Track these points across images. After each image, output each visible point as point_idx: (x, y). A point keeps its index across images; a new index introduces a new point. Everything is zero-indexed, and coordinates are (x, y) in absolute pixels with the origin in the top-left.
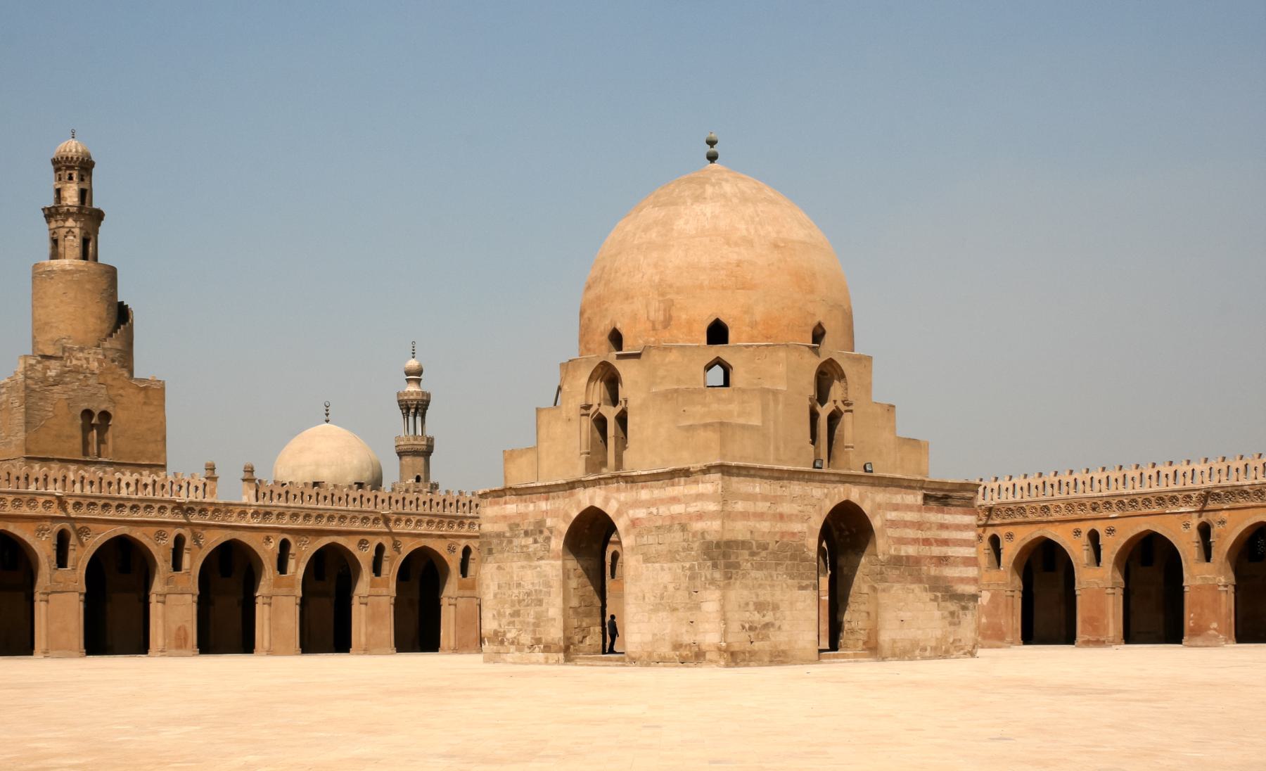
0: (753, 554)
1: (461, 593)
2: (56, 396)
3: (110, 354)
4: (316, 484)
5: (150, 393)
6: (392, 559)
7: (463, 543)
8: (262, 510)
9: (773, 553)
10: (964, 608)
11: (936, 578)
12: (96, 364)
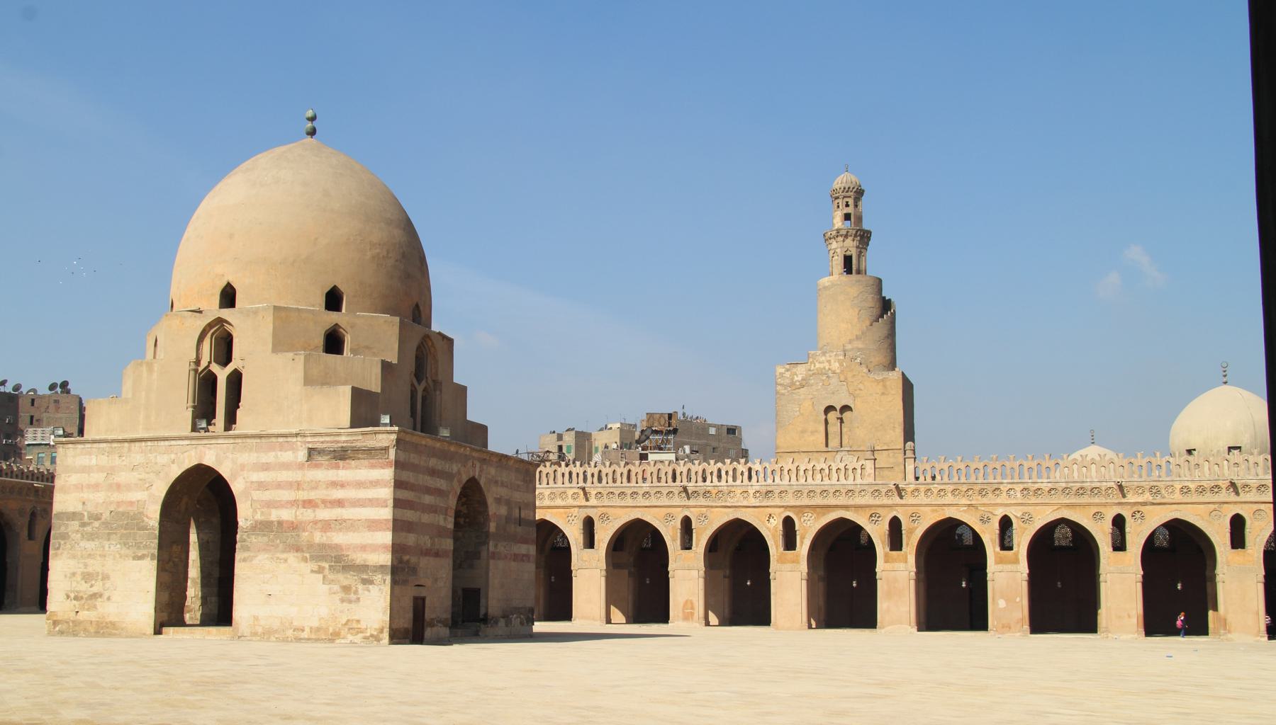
0: (83, 525)
1: (1000, 567)
3: (850, 354)
4: (1190, 452)
6: (911, 531)
7: (1000, 512)
8: (764, 490)
9: (106, 524)
10: (367, 582)
11: (323, 546)
12: (837, 364)
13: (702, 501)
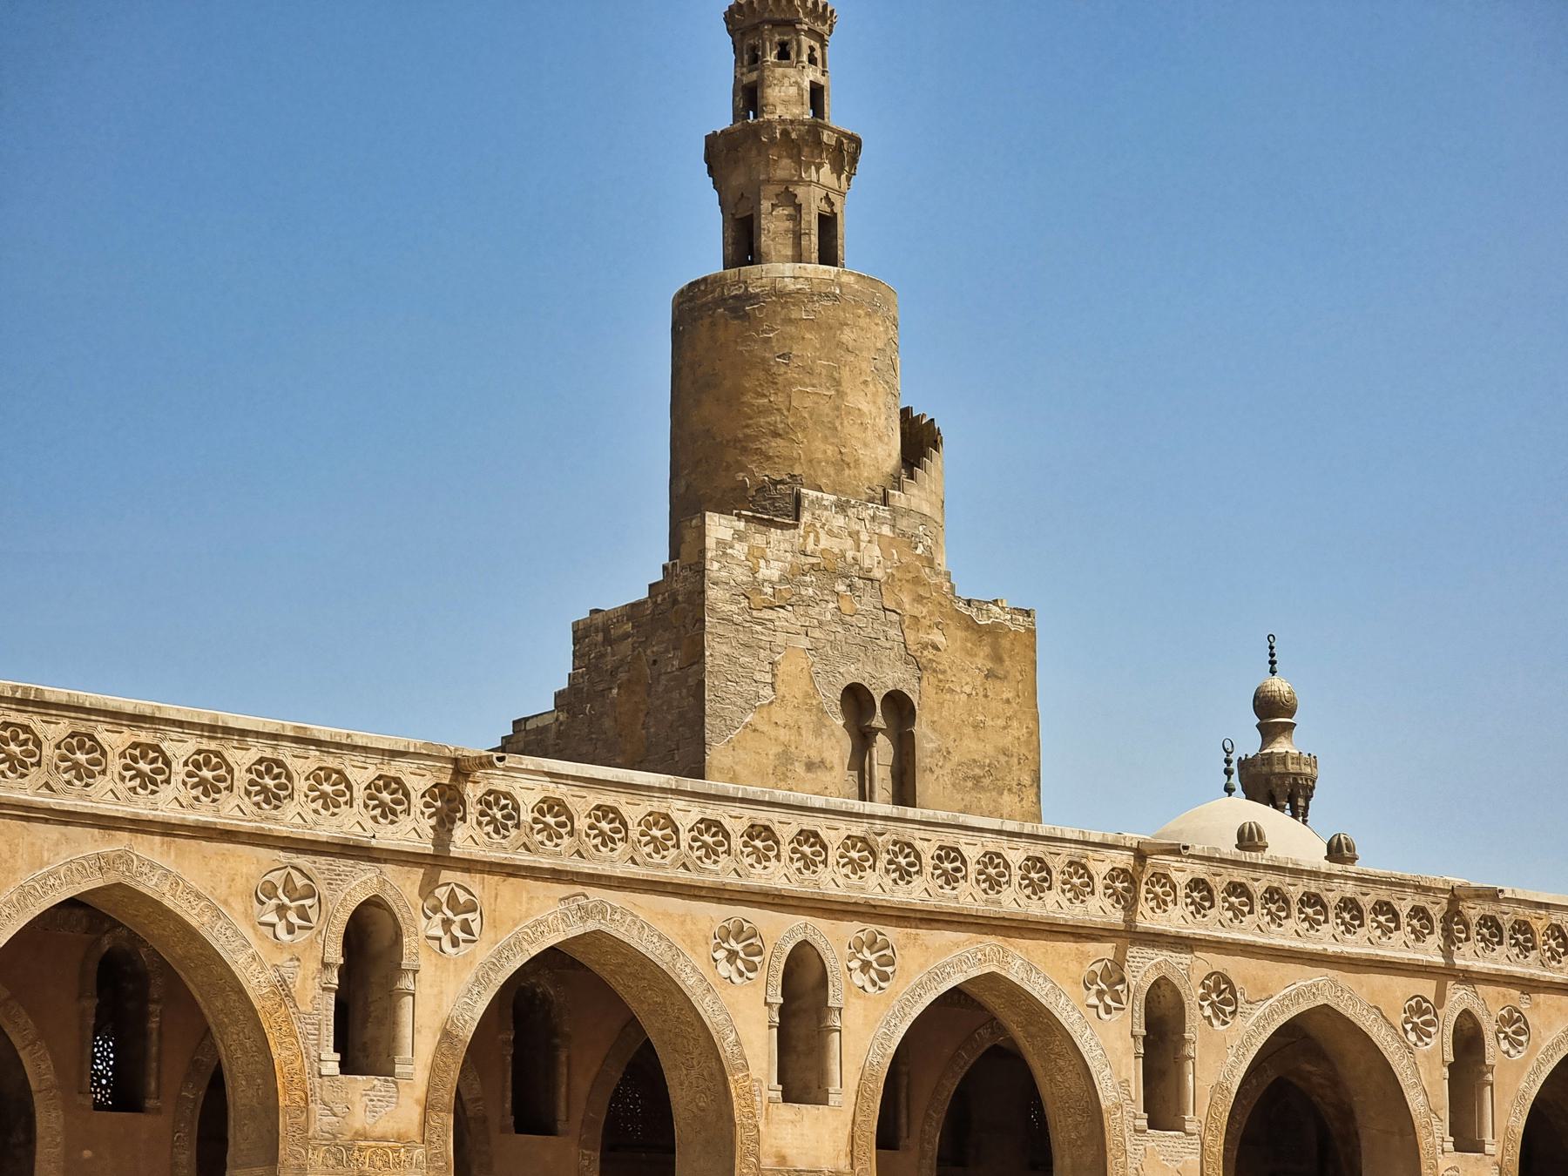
2: (780, 638)
5: (1005, 643)
12: (877, 552)
13: (1502, 960)
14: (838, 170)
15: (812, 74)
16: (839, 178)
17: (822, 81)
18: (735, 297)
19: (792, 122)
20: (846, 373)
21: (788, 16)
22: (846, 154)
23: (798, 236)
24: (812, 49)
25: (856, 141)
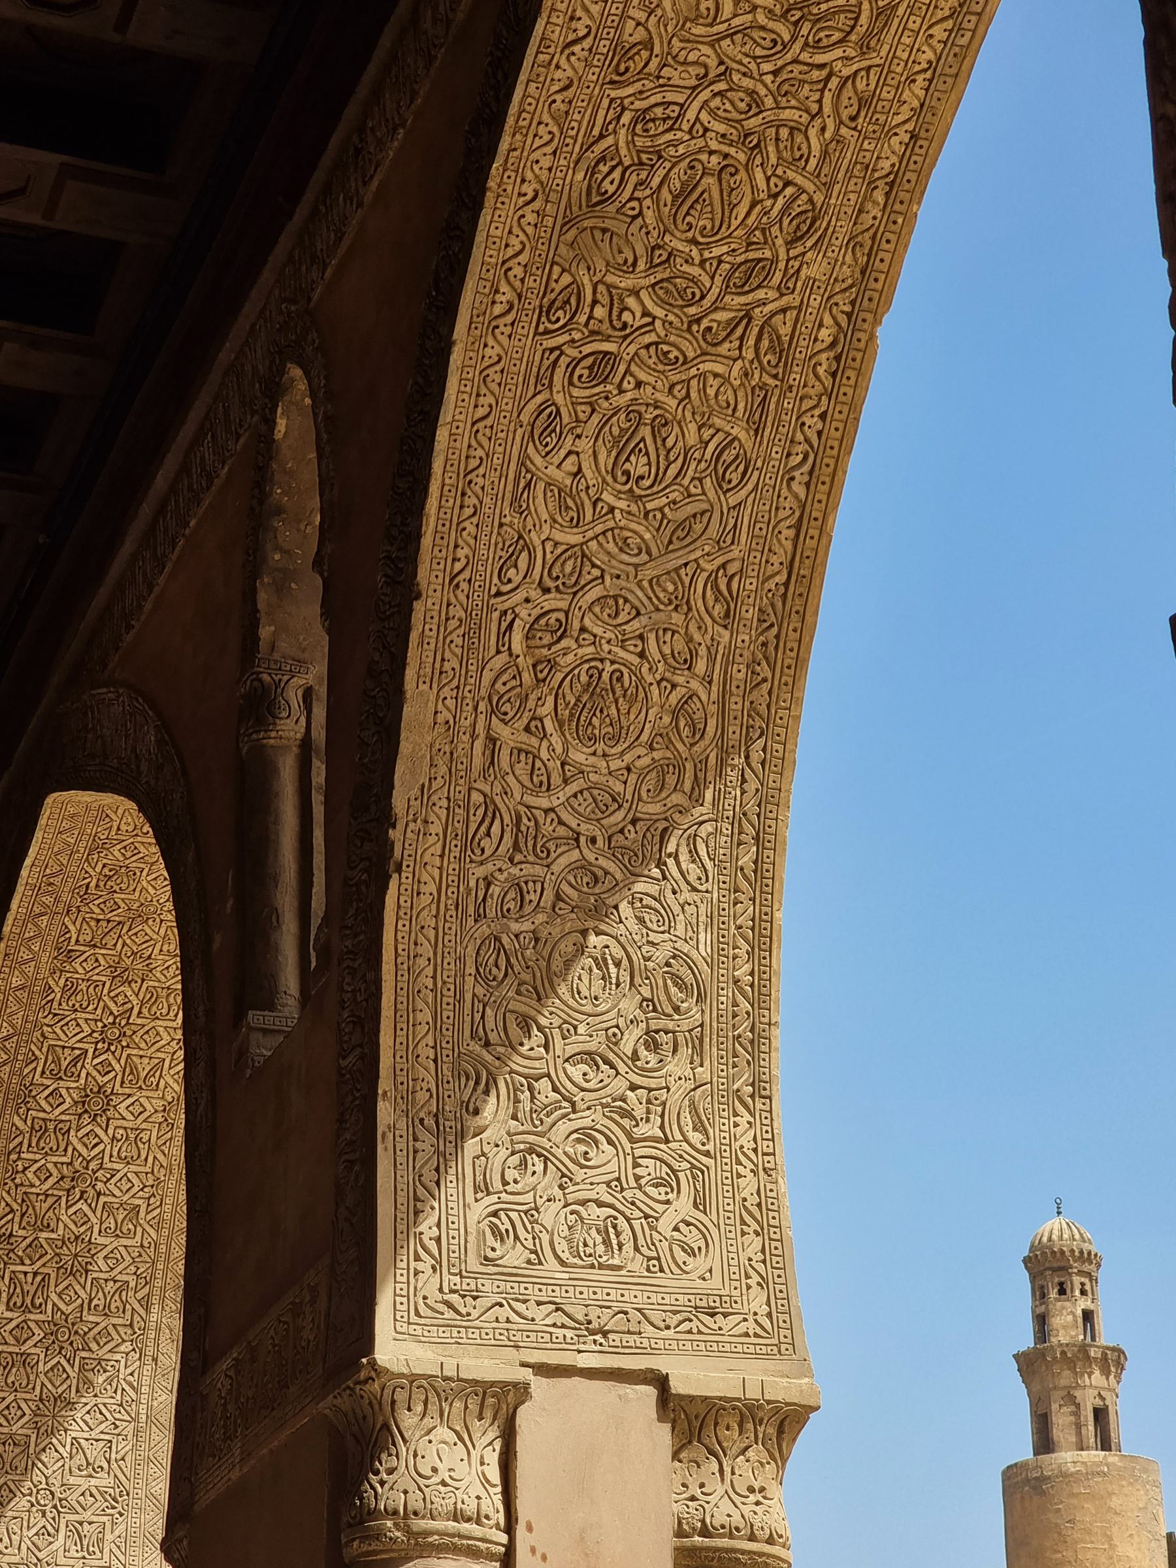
14: (1106, 1372)
15: (1083, 1304)
16: (1107, 1379)
17: (1092, 1307)
18: (1036, 1478)
19: (1067, 1345)
20: (1115, 1529)
21: (1063, 1264)
22: (1113, 1361)
23: (1079, 1427)
24: (1083, 1284)
25: (1120, 1352)
